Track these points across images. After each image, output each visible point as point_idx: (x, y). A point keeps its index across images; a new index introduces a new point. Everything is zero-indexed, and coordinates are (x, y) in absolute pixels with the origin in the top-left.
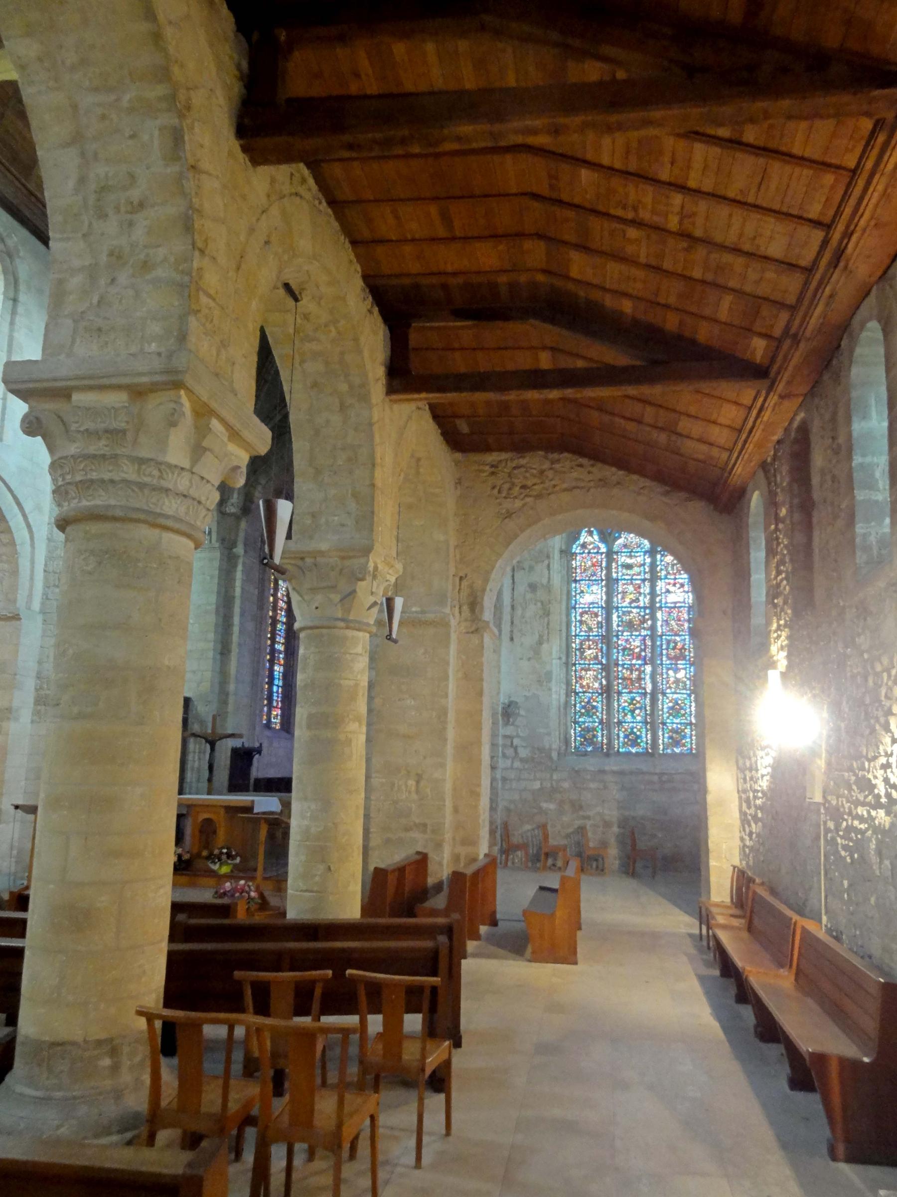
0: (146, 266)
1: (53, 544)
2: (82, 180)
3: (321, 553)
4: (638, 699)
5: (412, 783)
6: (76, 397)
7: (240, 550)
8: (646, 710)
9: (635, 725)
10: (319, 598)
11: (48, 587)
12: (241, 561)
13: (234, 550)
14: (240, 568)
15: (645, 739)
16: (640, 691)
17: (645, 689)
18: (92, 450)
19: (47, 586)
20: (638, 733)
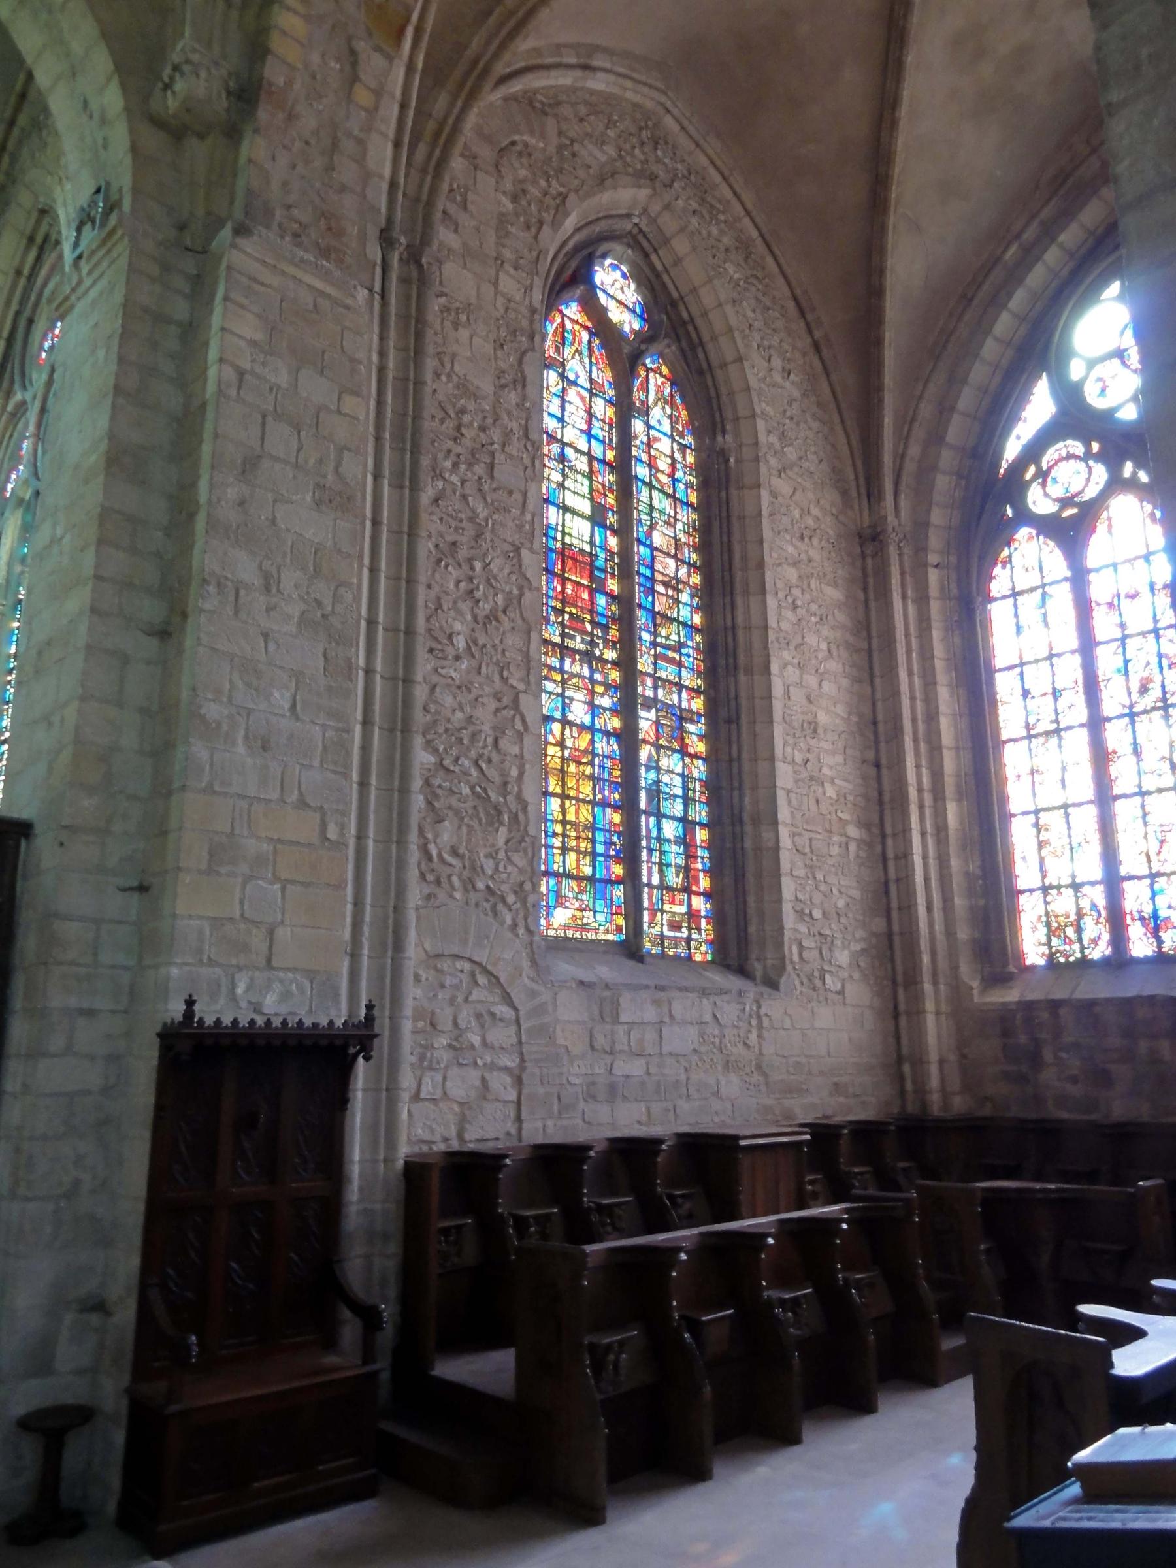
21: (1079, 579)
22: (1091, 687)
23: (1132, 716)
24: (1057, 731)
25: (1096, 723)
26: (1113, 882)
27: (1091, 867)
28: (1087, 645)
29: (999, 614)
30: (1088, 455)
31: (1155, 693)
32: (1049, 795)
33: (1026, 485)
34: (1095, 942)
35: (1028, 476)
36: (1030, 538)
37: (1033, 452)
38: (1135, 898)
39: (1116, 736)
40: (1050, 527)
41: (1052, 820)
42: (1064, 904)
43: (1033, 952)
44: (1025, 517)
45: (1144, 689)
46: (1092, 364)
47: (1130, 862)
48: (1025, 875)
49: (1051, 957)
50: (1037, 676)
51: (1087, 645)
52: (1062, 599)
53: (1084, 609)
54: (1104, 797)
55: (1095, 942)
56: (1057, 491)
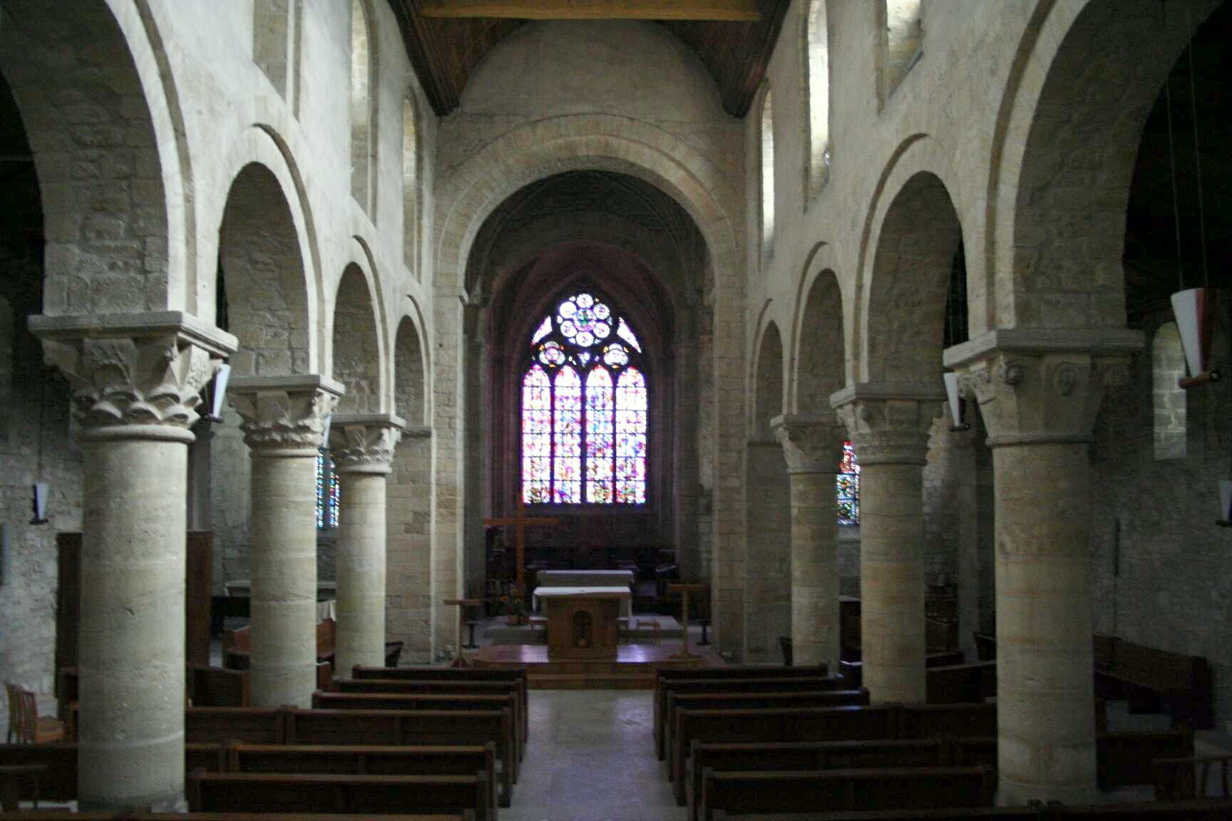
0: (918, 333)
1: (438, 367)
2: (891, 289)
3: (823, 424)
4: (849, 479)
5: (777, 565)
6: (889, 403)
7: (480, 338)
8: (855, 489)
9: (845, 501)
10: (819, 453)
11: (439, 406)
12: (483, 350)
13: (476, 340)
14: (482, 357)
15: (853, 513)
16: (850, 472)
17: (854, 470)
18: (899, 429)
19: (438, 405)
20: (849, 508)
21: (552, 389)
22: (552, 422)
23: (563, 434)
24: (541, 434)
25: (552, 434)
26: (552, 481)
27: (546, 476)
28: (553, 409)
29: (526, 391)
30: (558, 350)
31: (570, 429)
32: (535, 452)
33: (540, 352)
34: (545, 497)
35: (541, 349)
36: (539, 370)
37: (543, 341)
38: (557, 486)
39: (557, 438)
40: (545, 368)
41: (536, 460)
42: (537, 486)
43: (526, 500)
44: (538, 362)
45: (567, 427)
46: (564, 320)
47: (557, 476)
48: (526, 476)
49: (532, 501)
50: (537, 416)
51: (553, 409)
52: (547, 393)
53: (553, 398)
54: (552, 456)
55: (545, 497)
56: (549, 357)
